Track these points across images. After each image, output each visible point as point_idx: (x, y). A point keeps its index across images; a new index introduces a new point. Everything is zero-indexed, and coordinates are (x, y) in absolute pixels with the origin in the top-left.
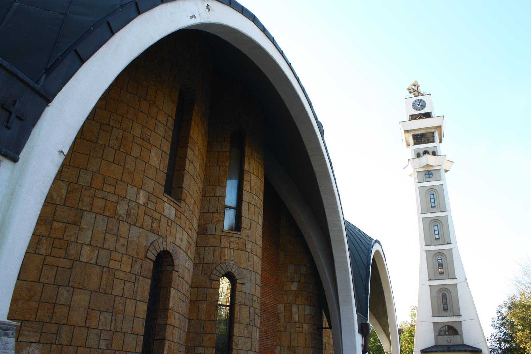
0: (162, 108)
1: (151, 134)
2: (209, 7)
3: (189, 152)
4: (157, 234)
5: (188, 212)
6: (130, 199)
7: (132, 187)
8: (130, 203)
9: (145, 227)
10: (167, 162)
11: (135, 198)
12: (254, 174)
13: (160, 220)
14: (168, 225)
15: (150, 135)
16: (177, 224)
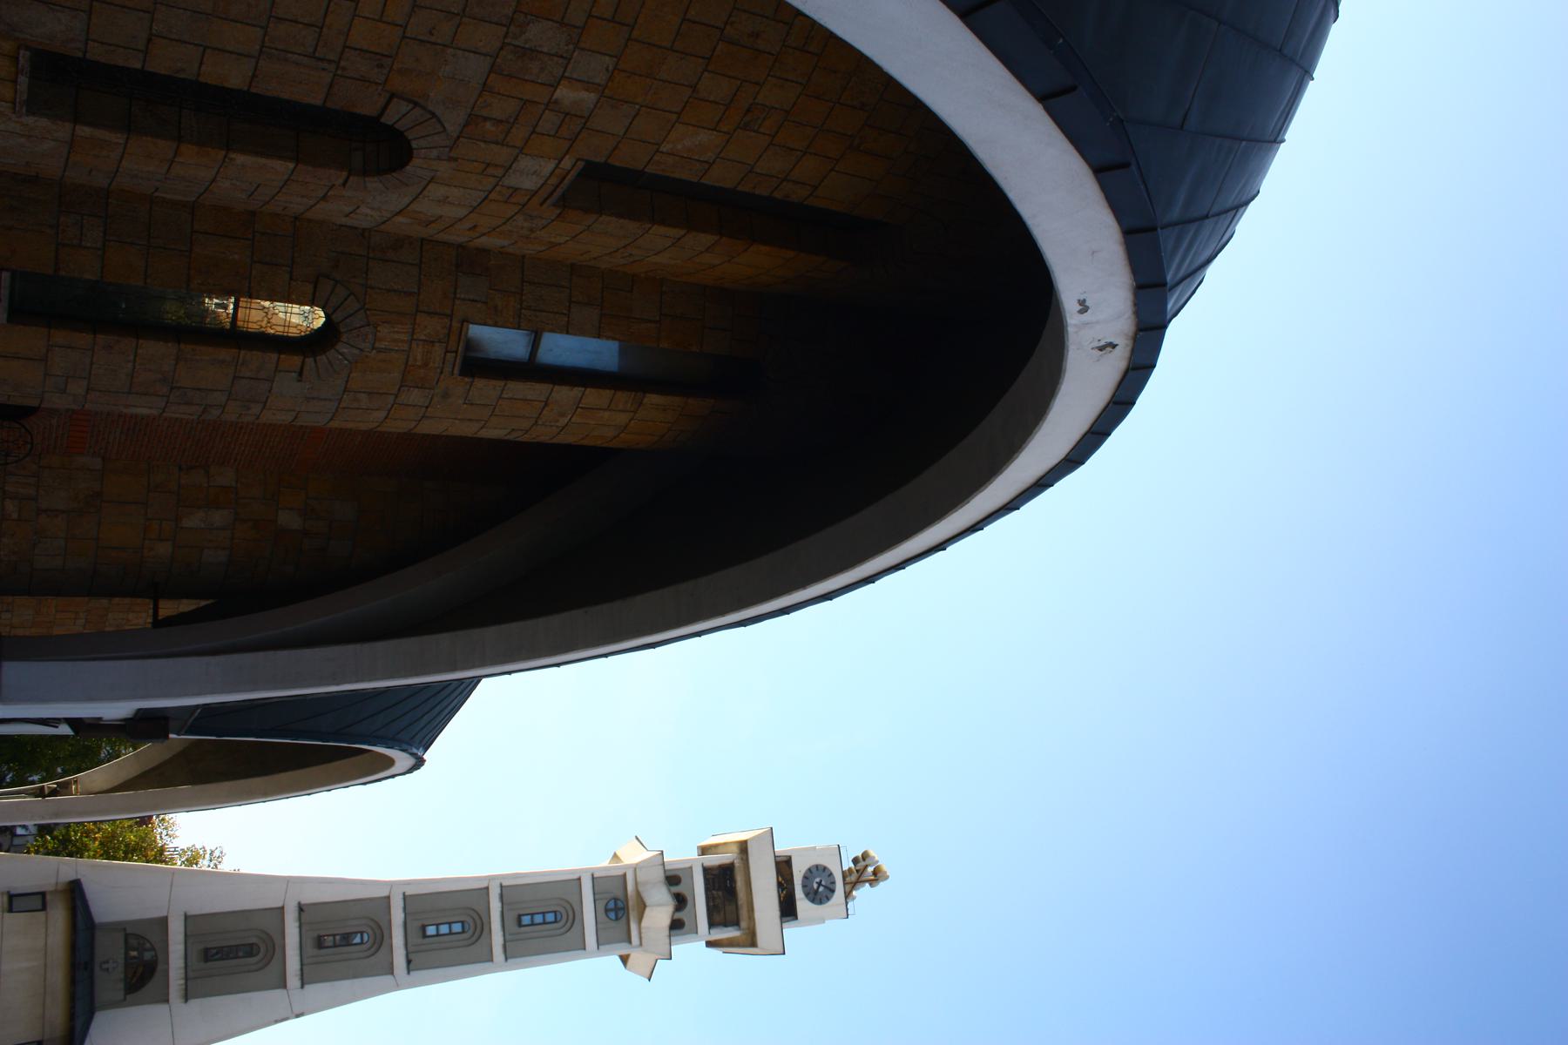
0: (837, 172)
1: (764, 134)
2: (1109, 349)
3: (707, 239)
4: (461, 132)
5: (526, 224)
6: (572, 61)
7: (607, 70)
8: (561, 61)
9: (485, 101)
10: (677, 176)
11: (575, 76)
12: (630, 421)
13: (503, 145)
14: (488, 165)
15: (762, 130)
16: (490, 192)
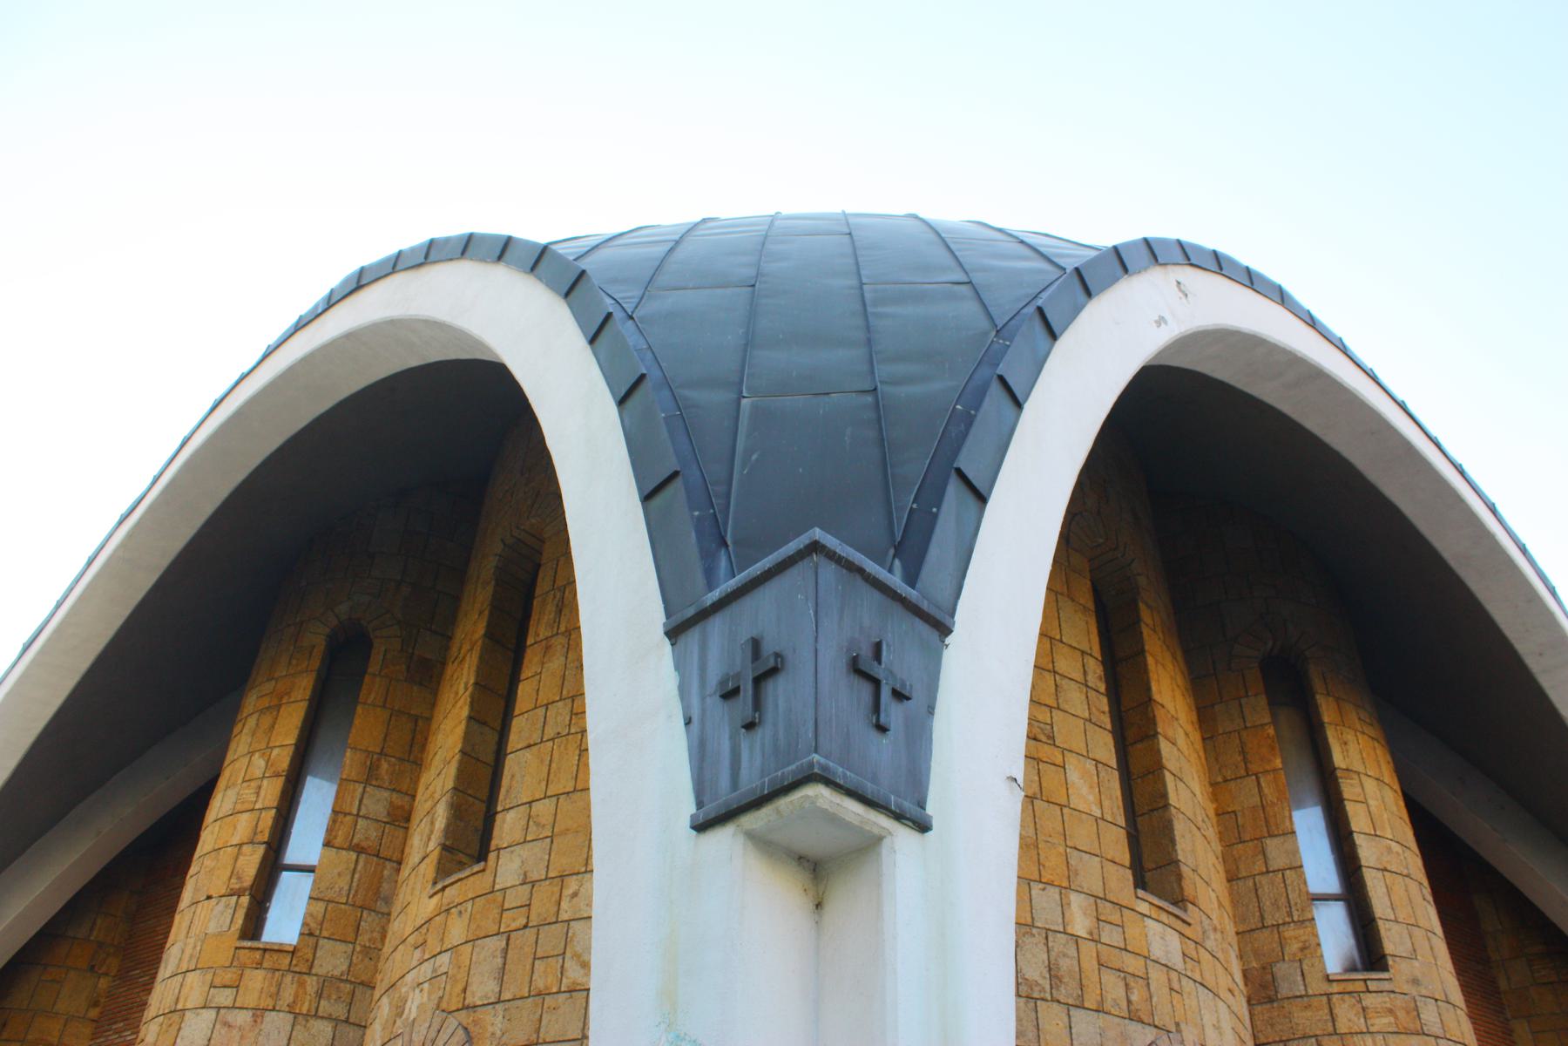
0: (1061, 636)
1: (1052, 718)
2: (1182, 287)
3: (1165, 747)
4: (1149, 1025)
5: (1212, 937)
6: (1047, 927)
7: (1044, 889)
8: (1050, 939)
9: (1112, 1007)
10: (1119, 793)
11: (1060, 920)
12: (1369, 776)
13: (1148, 979)
14: (1171, 989)
15: (1049, 722)
16: (1195, 981)
